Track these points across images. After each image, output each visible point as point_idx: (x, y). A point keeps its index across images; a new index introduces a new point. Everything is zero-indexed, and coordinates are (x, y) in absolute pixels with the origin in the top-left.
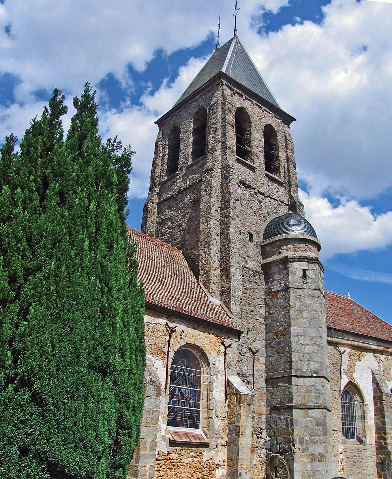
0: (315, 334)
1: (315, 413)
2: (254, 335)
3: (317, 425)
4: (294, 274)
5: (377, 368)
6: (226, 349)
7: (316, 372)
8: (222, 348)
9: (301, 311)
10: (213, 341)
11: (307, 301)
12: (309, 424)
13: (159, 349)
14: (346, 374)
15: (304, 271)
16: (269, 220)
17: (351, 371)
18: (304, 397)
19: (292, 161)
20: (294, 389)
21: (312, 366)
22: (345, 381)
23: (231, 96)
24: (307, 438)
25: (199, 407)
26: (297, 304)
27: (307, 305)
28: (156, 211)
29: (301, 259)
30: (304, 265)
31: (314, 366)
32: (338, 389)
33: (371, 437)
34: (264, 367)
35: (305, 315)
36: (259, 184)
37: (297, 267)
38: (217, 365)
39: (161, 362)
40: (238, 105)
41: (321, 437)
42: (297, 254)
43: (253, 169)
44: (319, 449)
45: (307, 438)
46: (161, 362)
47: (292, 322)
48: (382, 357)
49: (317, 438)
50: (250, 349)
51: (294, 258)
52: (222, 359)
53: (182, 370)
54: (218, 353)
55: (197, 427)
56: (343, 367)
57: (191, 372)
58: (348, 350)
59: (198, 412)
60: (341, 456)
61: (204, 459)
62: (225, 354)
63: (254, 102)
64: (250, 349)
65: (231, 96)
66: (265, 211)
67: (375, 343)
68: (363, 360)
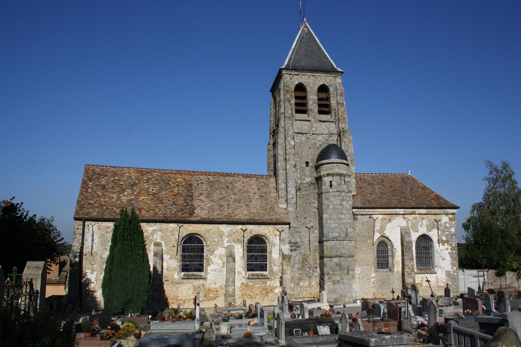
0: (336, 217)
1: (336, 260)
2: (310, 219)
3: (336, 266)
4: (325, 184)
5: (406, 225)
7: (336, 238)
8: (278, 233)
9: (328, 205)
10: (271, 231)
11: (332, 199)
12: (332, 266)
13: (238, 240)
14: (379, 232)
15: (331, 182)
16: (321, 149)
17: (383, 228)
18: (330, 252)
19: (340, 103)
20: (325, 247)
21: (334, 235)
22: (377, 236)
23: (291, 79)
24: (331, 272)
25: (266, 261)
26: (326, 201)
27: (332, 202)
28: (272, 149)
29: (328, 175)
30: (330, 178)
31: (336, 234)
32: (371, 241)
33: (398, 268)
34: (318, 235)
35: (331, 207)
37: (327, 180)
38: (274, 241)
39: (240, 246)
40: (297, 83)
41: (339, 272)
42: (327, 172)
43: (309, 121)
44: (338, 278)
45: (331, 272)
46: (240, 246)
47: (324, 212)
48: (411, 217)
49: (336, 272)
50: (307, 227)
51: (324, 175)
52: (278, 238)
54: (275, 235)
55: (266, 270)
56: (376, 228)
57: (260, 246)
58: (381, 217)
59: (266, 264)
60: (373, 279)
63: (308, 74)
64: (307, 227)
65: (291, 79)
66: (318, 144)
67: (402, 210)
68: (393, 222)
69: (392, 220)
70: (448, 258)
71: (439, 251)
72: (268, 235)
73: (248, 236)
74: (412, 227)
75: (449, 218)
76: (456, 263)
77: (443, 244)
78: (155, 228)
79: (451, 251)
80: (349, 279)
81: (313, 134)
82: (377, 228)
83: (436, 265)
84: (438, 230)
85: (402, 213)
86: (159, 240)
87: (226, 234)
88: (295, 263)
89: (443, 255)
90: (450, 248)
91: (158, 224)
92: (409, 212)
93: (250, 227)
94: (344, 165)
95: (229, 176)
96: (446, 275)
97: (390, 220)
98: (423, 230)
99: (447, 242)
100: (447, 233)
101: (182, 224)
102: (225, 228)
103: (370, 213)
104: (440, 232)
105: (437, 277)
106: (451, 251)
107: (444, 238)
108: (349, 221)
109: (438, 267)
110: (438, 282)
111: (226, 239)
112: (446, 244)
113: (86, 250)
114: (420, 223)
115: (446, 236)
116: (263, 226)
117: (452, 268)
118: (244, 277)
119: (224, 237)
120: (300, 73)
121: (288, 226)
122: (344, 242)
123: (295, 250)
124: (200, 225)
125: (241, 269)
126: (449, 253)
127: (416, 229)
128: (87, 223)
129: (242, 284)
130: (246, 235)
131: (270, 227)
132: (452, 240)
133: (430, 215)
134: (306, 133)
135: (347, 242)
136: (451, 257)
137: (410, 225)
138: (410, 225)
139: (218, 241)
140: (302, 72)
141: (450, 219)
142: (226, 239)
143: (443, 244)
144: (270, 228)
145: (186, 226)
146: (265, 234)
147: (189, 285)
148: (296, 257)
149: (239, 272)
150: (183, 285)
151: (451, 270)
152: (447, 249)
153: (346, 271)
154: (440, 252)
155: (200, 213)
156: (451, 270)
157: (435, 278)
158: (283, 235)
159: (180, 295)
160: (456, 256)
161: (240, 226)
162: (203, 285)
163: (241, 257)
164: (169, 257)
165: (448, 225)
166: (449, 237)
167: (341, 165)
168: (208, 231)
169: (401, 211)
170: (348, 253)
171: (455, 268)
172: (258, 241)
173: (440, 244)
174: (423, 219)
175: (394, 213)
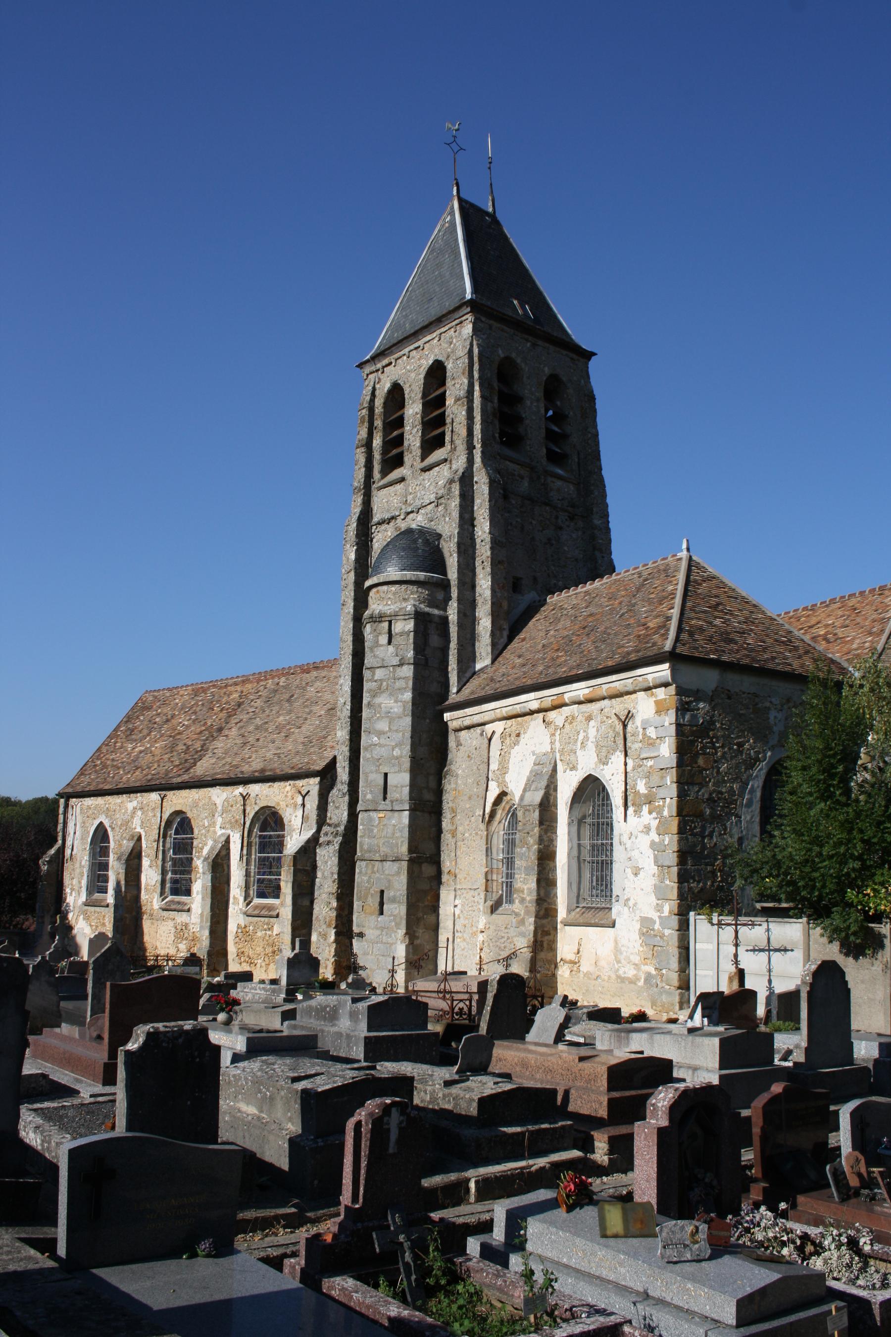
6: (304, 797)
10: (290, 794)
17: (504, 769)
36: (410, 498)
53: (270, 836)
58: (499, 727)
60: (481, 937)
61: (275, 933)
62: (303, 805)
63: (406, 350)
67: (532, 695)
68: (523, 739)
69: (522, 736)
70: (649, 867)
71: (625, 838)
72: (283, 804)
73: (251, 814)
74: (562, 752)
75: (657, 703)
76: (671, 885)
77: (638, 812)
78: (135, 803)
79: (657, 839)
80: (382, 929)
81: (408, 513)
82: (494, 766)
83: (615, 892)
84: (626, 755)
85: (535, 705)
86: (138, 830)
87: (220, 808)
88: (324, 878)
89: (635, 854)
90: (654, 824)
91: (139, 795)
92: (548, 703)
93: (254, 789)
94: (393, 588)
95: (316, 668)
96: (642, 934)
97: (518, 735)
98: (587, 763)
99: (649, 800)
100: (650, 763)
101: (164, 793)
102: (219, 795)
103: (477, 719)
104: (630, 762)
105: (616, 942)
106: (657, 839)
107: (642, 787)
108: (397, 752)
109: (622, 901)
110: (619, 962)
111: (219, 821)
112: (645, 809)
113: (68, 852)
114: (581, 737)
115: (648, 776)
116: (277, 785)
117: (659, 909)
118: (241, 909)
119: (217, 815)
120: (391, 359)
121: (318, 779)
122: (374, 815)
123: (329, 843)
124: (194, 791)
125: (238, 891)
126: (653, 845)
127: (572, 758)
128: (73, 801)
129: (239, 926)
130: (248, 809)
131: (287, 787)
132: (662, 793)
133: (606, 702)
134: (393, 518)
135: (381, 815)
136: (656, 862)
137: (557, 745)
138: (557, 745)
139: (210, 825)
140: (392, 353)
141: (660, 708)
142: (219, 821)
143: (638, 812)
144: (288, 788)
145: (170, 794)
146: (278, 804)
147: (171, 924)
148: (326, 862)
149: (234, 898)
150: (164, 923)
151: (655, 916)
152: (647, 829)
153: (374, 902)
154: (629, 844)
155: (203, 768)
156: (655, 916)
157: (611, 945)
158: (308, 806)
159: (158, 944)
160: (671, 858)
161: (240, 789)
162: (186, 925)
163: (239, 866)
164: (149, 863)
165: (652, 733)
166: (655, 779)
167: (385, 588)
168: (196, 804)
169: (531, 700)
170: (384, 850)
171: (667, 909)
172: (276, 822)
173: (631, 810)
174: (589, 718)
175: (518, 709)
